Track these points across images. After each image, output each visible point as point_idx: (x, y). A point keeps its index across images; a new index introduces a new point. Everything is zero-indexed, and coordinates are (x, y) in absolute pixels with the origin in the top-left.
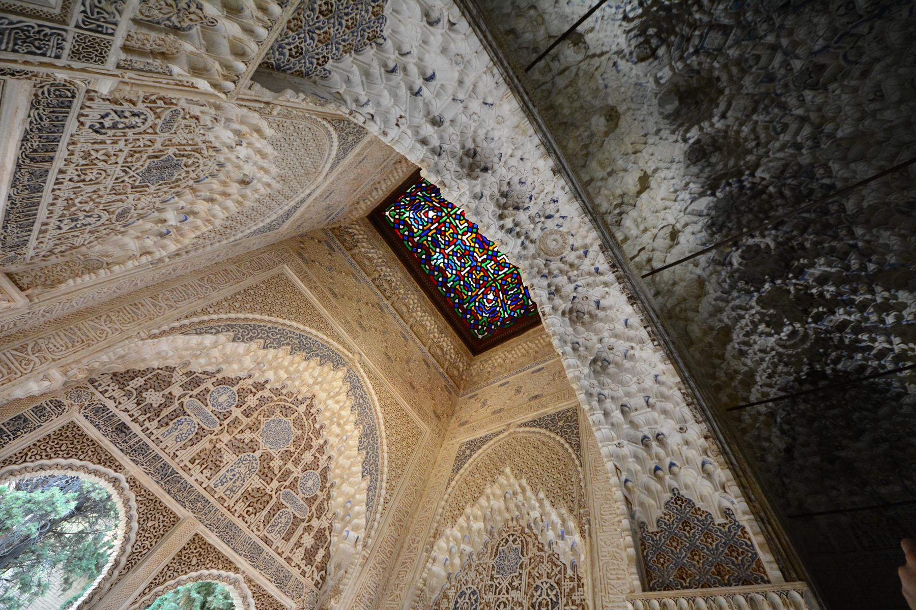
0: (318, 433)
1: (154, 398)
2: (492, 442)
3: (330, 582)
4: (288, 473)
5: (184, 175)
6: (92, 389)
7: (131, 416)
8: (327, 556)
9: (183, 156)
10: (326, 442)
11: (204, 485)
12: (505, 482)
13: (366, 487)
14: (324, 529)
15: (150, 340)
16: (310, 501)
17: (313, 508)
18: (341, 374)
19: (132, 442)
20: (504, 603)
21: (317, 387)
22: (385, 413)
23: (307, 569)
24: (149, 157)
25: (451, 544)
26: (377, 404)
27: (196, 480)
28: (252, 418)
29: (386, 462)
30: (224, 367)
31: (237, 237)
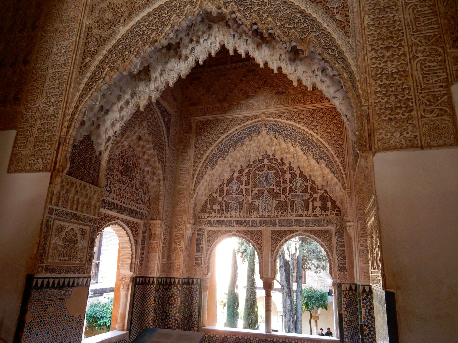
0: (283, 164)
1: (217, 207)
3: (343, 211)
4: (285, 190)
5: (131, 162)
6: (202, 220)
8: (334, 203)
9: (123, 163)
11: (258, 217)
16: (305, 190)
17: (309, 191)
19: (226, 223)
22: (305, 124)
23: (327, 212)
24: (122, 176)
27: (254, 217)
29: (327, 146)
30: (221, 178)
31: (167, 141)
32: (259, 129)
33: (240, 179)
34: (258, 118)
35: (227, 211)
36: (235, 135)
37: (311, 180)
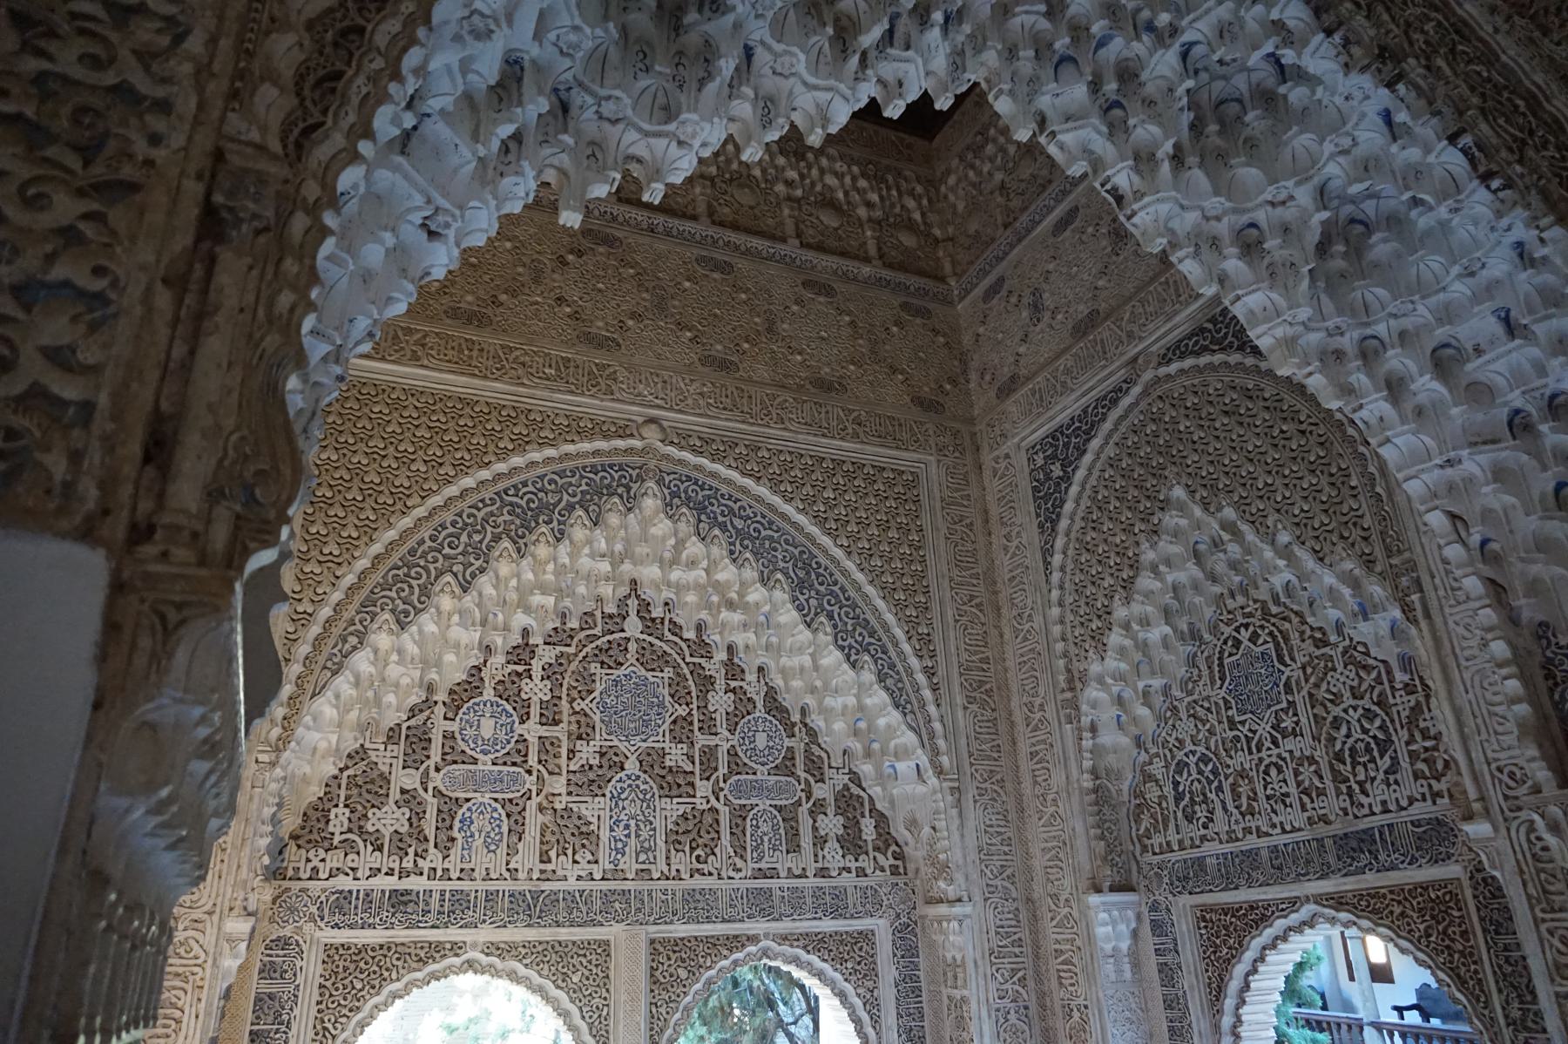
0: (702, 646)
1: (389, 819)
2: (1107, 426)
3: (916, 853)
4: (709, 754)
6: (296, 886)
7: (390, 873)
8: (881, 820)
10: (730, 649)
11: (597, 876)
12: (1183, 522)
13: (873, 678)
14: (846, 788)
15: (286, 754)
16: (786, 767)
18: (650, 504)
20: (1276, 765)
21: (627, 567)
22: (807, 505)
23: (864, 862)
25: (1115, 689)
26: (777, 500)
27: (579, 878)
28: (565, 718)
29: (880, 604)
30: (433, 675)
32: (635, 486)
33: (513, 690)
34: (632, 435)
35: (445, 847)
36: (525, 484)
37: (806, 725)
